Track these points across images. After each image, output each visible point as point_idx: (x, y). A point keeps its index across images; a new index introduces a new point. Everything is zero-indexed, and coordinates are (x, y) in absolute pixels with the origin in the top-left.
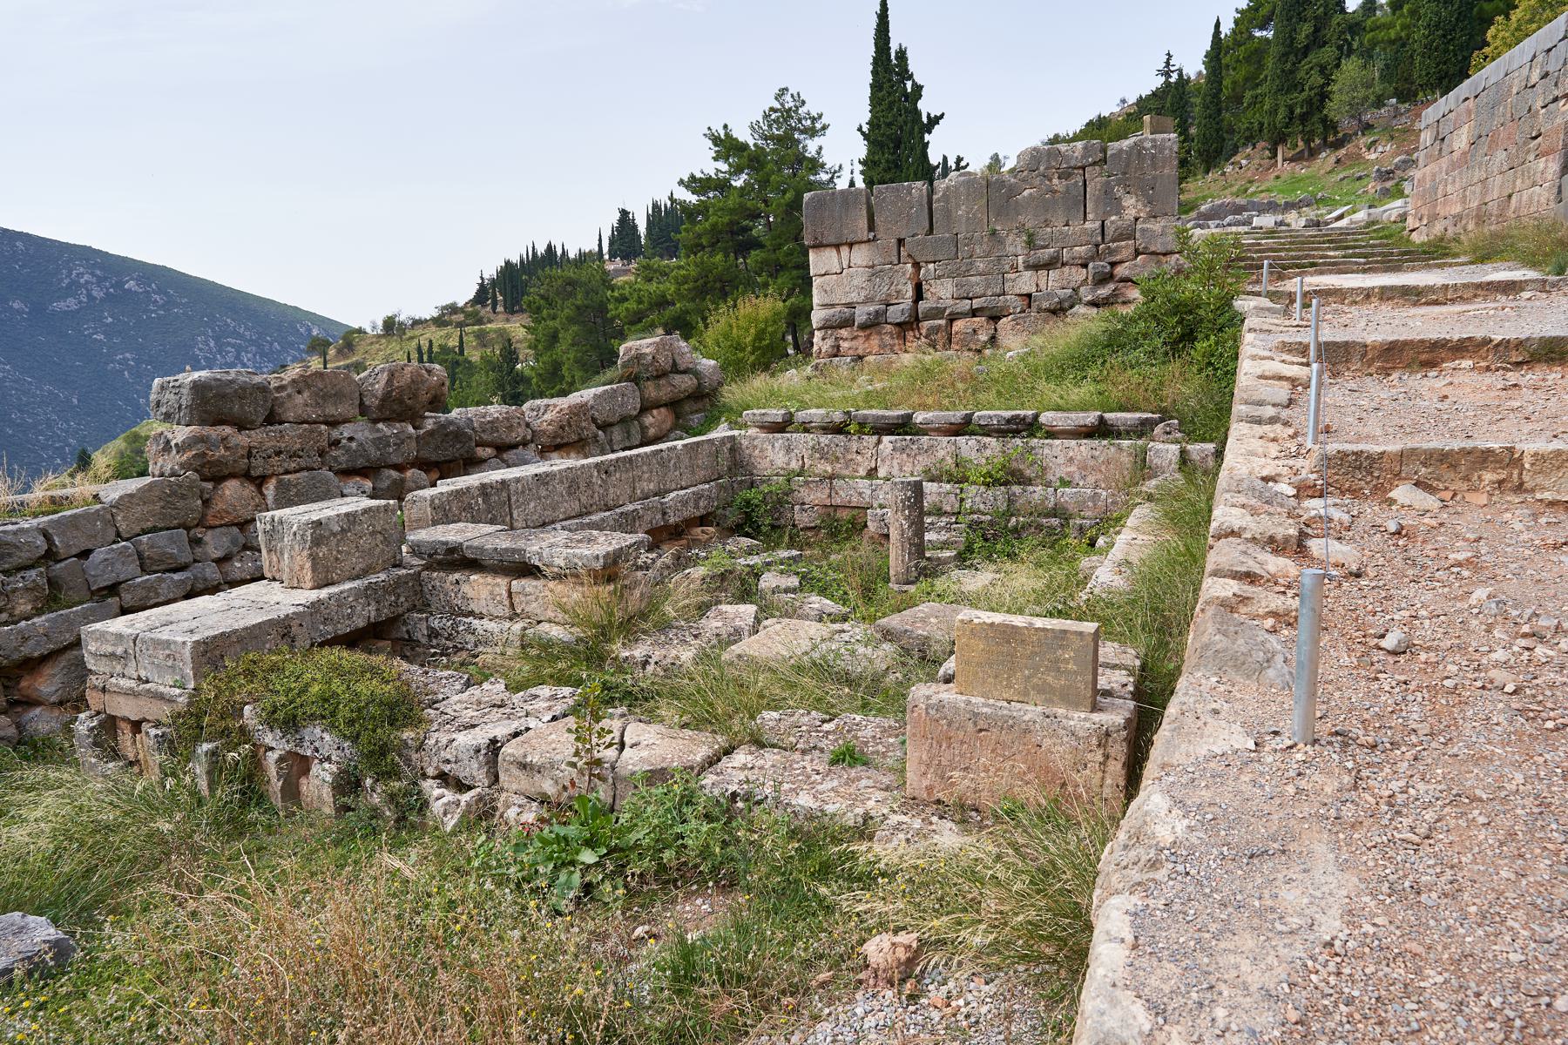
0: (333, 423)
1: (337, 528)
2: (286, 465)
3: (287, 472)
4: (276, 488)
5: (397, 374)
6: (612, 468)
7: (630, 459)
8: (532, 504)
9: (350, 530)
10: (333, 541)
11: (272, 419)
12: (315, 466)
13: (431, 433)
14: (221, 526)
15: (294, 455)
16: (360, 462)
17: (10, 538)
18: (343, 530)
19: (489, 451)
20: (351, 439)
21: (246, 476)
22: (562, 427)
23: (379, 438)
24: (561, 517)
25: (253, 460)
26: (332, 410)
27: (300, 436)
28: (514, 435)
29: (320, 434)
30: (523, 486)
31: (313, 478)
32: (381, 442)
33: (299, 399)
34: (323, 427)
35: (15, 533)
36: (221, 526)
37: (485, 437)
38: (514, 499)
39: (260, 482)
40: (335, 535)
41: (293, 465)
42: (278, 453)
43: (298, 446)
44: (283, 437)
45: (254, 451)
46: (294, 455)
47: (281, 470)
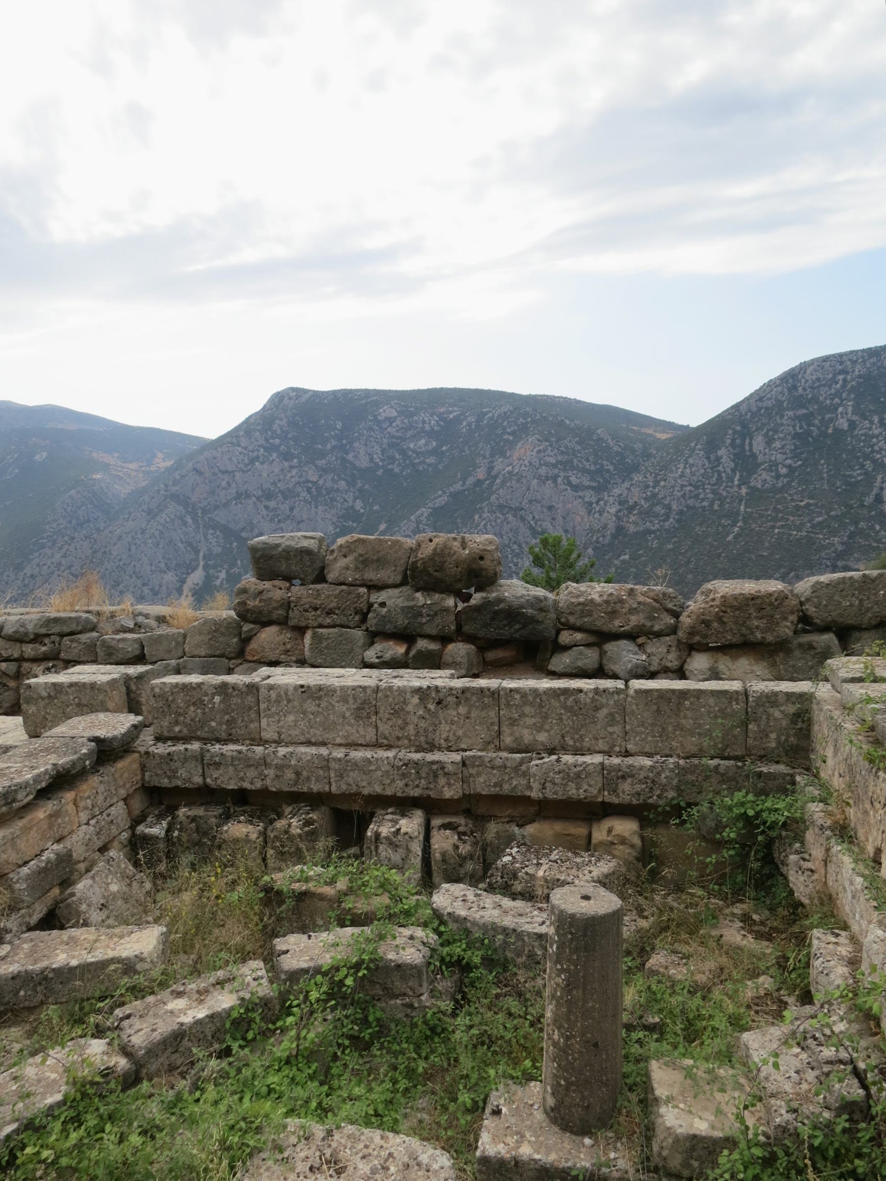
0: (375, 587)
1: (44, 694)
2: (320, 620)
3: (321, 626)
4: (313, 638)
5: (423, 545)
6: (451, 699)
7: (495, 694)
8: (291, 718)
9: (56, 698)
10: (42, 704)
11: (321, 578)
12: (351, 624)
13: (477, 609)
14: (253, 662)
15: (330, 612)
16: (389, 628)
17: (114, 643)
18: (49, 696)
19: (579, 636)
20: (383, 605)
21: (283, 622)
22: (707, 624)
23: (412, 607)
24: (338, 741)
25: (290, 612)
26: (372, 575)
27: (336, 597)
28: (617, 623)
29: (359, 596)
30: (279, 695)
31: (341, 636)
32: (414, 612)
33: (342, 562)
34: (363, 590)
35: (119, 640)
36: (253, 662)
37: (572, 619)
38: (263, 706)
39: (301, 630)
40: (42, 698)
41: (328, 621)
42: (316, 609)
43: (333, 605)
44: (318, 595)
45: (292, 605)
46: (330, 612)
47: (315, 624)
